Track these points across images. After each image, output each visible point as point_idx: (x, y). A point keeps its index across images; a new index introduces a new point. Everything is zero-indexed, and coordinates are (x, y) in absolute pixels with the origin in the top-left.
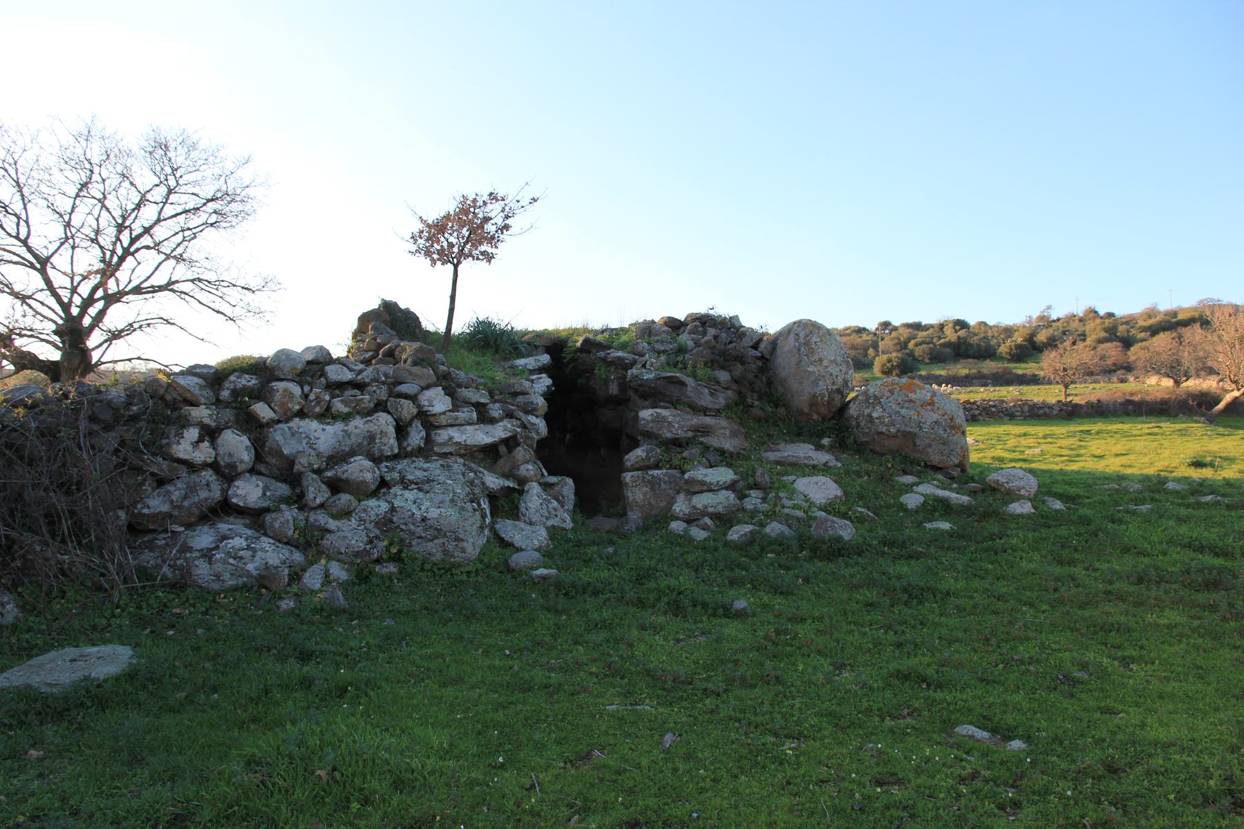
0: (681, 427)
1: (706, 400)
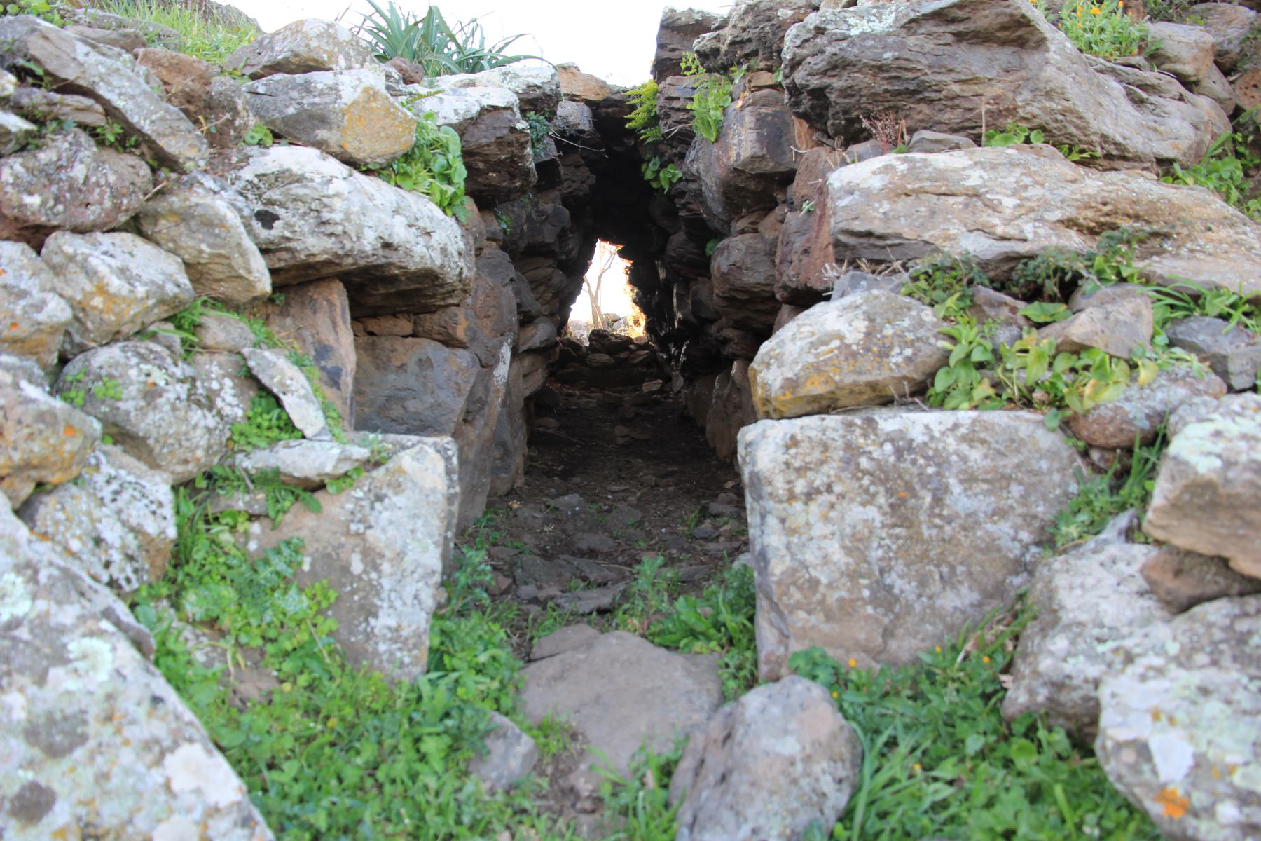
0: (1026, 210)
1: (1115, 118)
